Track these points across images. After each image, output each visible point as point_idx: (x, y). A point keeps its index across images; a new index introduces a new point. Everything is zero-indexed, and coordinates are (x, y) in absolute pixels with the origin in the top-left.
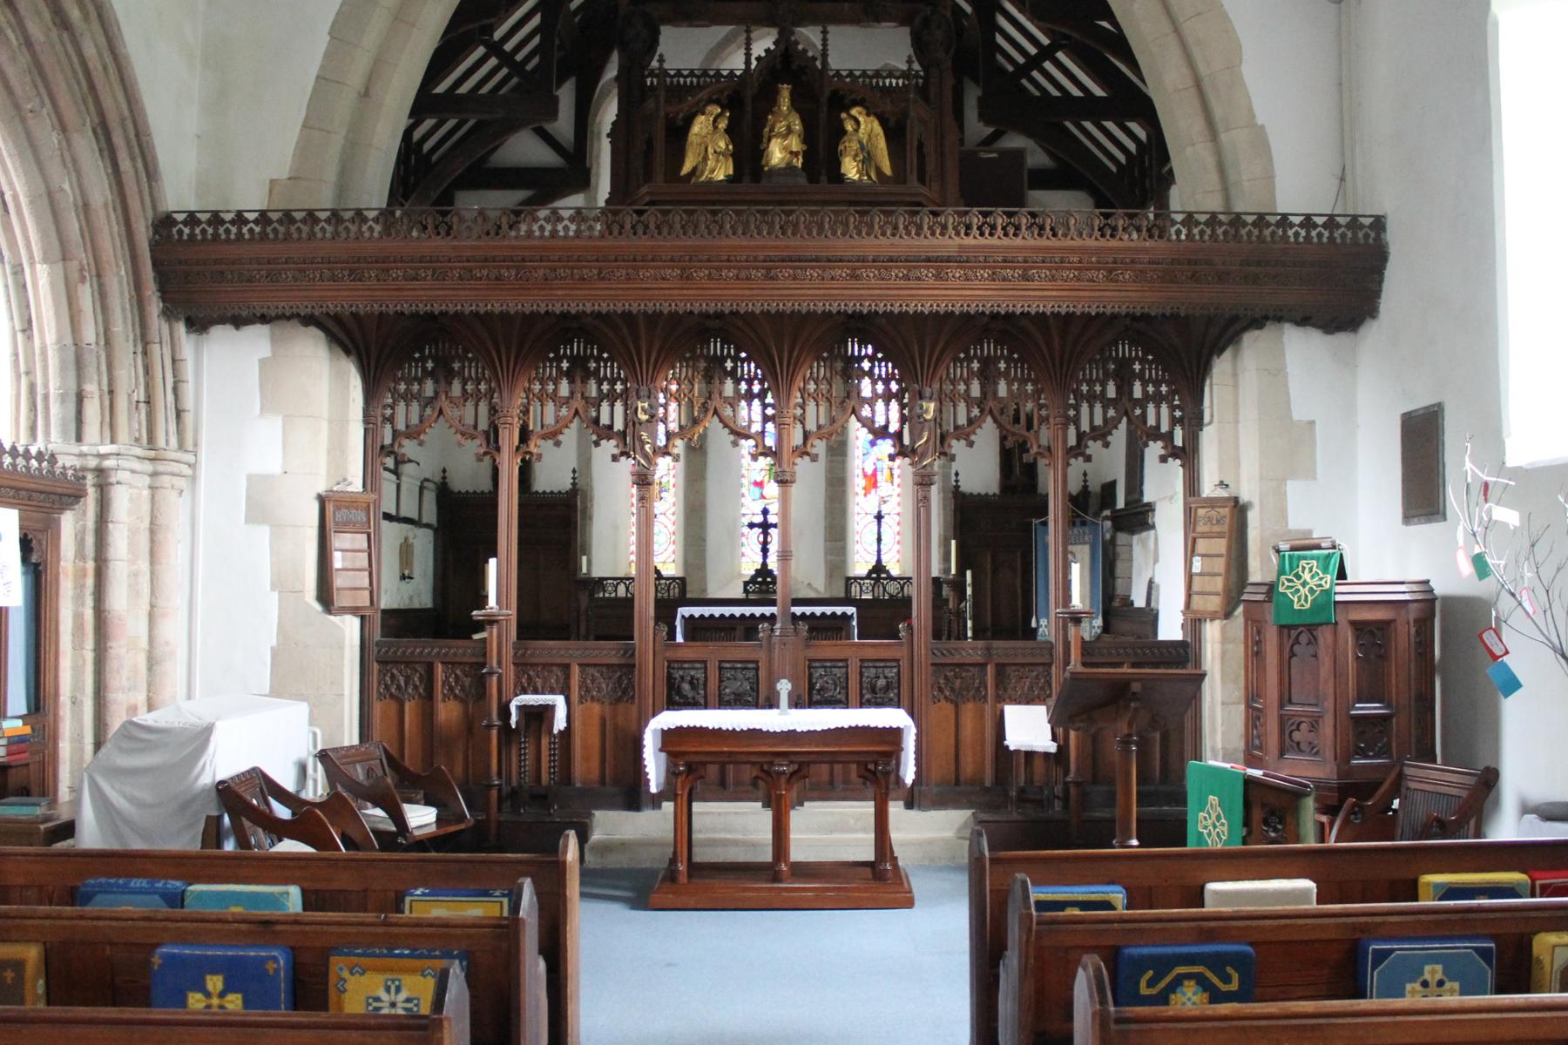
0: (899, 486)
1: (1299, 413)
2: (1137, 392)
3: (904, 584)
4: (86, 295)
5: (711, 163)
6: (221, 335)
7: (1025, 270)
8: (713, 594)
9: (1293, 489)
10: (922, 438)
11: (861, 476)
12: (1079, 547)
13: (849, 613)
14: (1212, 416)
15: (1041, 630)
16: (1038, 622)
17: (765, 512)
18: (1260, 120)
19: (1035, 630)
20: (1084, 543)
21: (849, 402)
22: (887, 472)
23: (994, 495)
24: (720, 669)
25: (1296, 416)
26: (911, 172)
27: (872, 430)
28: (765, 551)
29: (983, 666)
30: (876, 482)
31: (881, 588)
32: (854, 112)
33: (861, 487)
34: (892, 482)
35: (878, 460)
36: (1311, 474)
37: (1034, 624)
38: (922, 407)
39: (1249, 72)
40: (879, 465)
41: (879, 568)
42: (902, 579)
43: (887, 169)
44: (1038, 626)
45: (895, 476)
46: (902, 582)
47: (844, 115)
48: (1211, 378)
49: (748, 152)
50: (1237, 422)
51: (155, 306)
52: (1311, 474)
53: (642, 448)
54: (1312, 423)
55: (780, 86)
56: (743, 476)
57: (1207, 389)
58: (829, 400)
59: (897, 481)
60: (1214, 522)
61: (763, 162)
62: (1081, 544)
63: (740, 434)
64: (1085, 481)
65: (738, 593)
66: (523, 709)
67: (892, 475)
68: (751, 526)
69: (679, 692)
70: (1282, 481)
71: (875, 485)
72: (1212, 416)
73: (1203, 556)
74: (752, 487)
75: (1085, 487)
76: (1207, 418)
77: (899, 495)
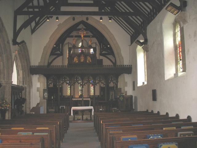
1: (126, 81)
2: (113, 79)
4: (24, 73)
6: (34, 75)
8: (76, 97)
17: (81, 89)
21: (89, 81)
28: (81, 93)
36: (127, 86)
39: (122, 52)
49: (79, 60)
51: (30, 73)
52: (127, 86)
63: (79, 83)
65: (78, 97)
66: (61, 107)
68: (80, 90)
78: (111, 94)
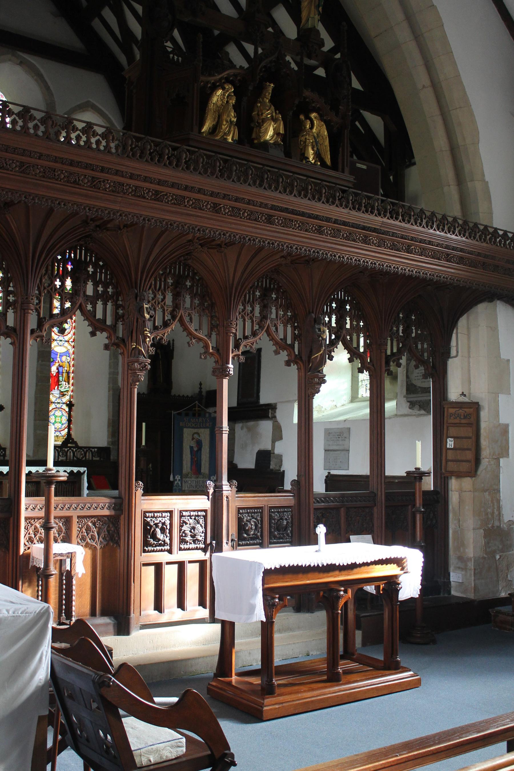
0: (72, 385)
3: (87, 451)
5: (225, 127)
7: (408, 246)
9: (502, 398)
10: (321, 351)
12: (202, 430)
13: (82, 472)
14: (457, 352)
15: (176, 482)
16: (174, 477)
18: (487, 178)
19: (172, 483)
20: (206, 427)
22: (65, 375)
23: (144, 394)
24: (181, 516)
25: (502, 357)
26: (347, 166)
27: (276, 343)
29: (337, 509)
30: (58, 381)
31: (72, 454)
32: (313, 115)
37: (171, 479)
38: (320, 330)
40: (61, 369)
41: (69, 439)
42: (85, 448)
43: (328, 162)
44: (175, 480)
45: (71, 378)
46: (85, 450)
47: (302, 117)
48: (457, 329)
50: (469, 357)
53: (144, 341)
54: (508, 361)
55: (268, 84)
57: (454, 336)
58: (251, 318)
59: (71, 381)
60: (462, 417)
61: (254, 136)
62: (204, 428)
64: (201, 388)
67: (68, 377)
69: (154, 536)
70: (497, 395)
72: (457, 352)
73: (454, 437)
75: (200, 392)
76: (453, 352)
78: (188, 443)
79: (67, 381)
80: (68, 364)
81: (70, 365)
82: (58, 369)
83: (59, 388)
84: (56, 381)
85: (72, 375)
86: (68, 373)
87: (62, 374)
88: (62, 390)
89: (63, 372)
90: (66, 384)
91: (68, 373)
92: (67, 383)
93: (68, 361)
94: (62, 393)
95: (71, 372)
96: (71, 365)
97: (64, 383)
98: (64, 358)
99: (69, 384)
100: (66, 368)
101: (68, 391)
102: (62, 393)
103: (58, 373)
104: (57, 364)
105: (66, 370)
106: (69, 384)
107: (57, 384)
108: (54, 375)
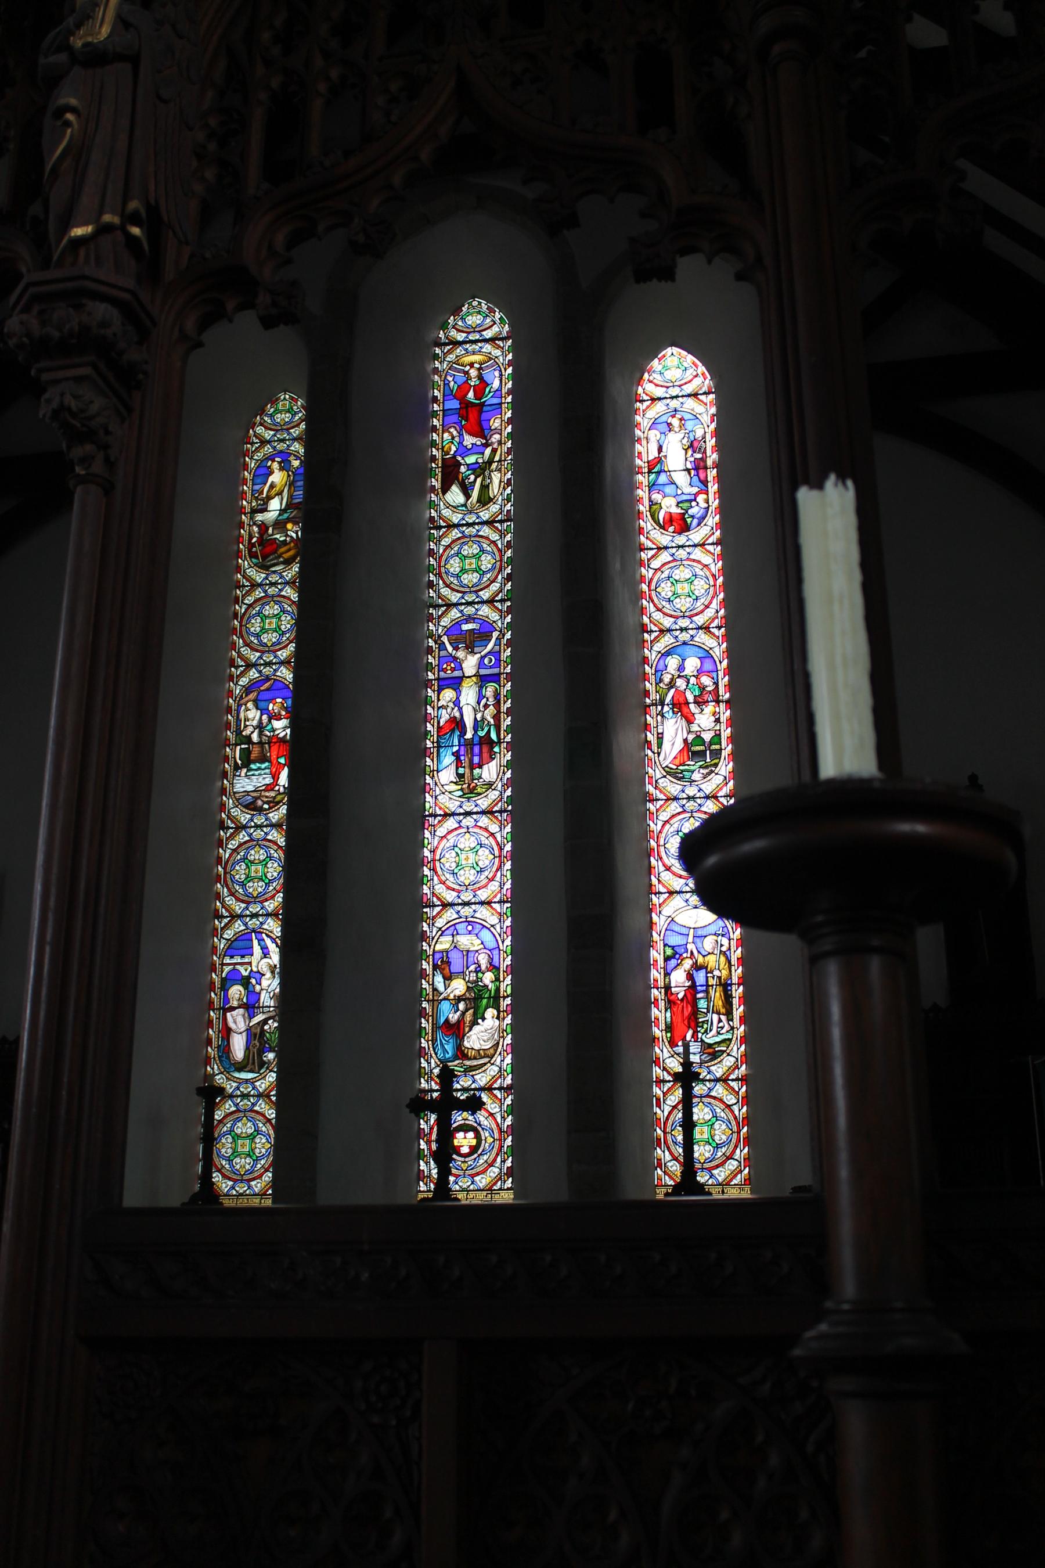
0: (742, 1020)
11: (662, 1004)
22: (717, 995)
30: (695, 1010)
33: (663, 1026)
34: (729, 1014)
35: (697, 967)
40: (700, 977)
45: (735, 1002)
56: (423, 1013)
59: (738, 1011)
67: (728, 998)
71: (694, 1021)
74: (439, 1035)
77: (743, 1040)
79: (723, 1011)
80: (723, 959)
81: (729, 962)
82: (690, 977)
83: (700, 1035)
84: (686, 1014)
85: (737, 992)
86: (725, 986)
87: (707, 992)
88: (710, 1039)
89: (707, 985)
90: (720, 1021)
91: (725, 986)
92: (723, 1018)
93: (724, 949)
94: (711, 1050)
95: (735, 980)
96: (734, 961)
97: (715, 1017)
98: (708, 944)
99: (730, 1019)
100: (717, 973)
101: (730, 1040)
102: (711, 1050)
103: (693, 988)
104: (688, 964)
105: (719, 978)
106: (730, 1019)
107: (693, 1024)
108: (680, 996)
